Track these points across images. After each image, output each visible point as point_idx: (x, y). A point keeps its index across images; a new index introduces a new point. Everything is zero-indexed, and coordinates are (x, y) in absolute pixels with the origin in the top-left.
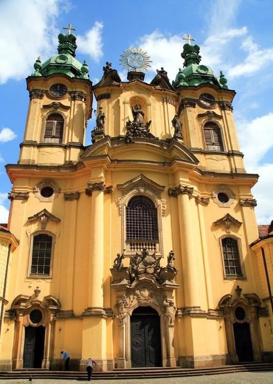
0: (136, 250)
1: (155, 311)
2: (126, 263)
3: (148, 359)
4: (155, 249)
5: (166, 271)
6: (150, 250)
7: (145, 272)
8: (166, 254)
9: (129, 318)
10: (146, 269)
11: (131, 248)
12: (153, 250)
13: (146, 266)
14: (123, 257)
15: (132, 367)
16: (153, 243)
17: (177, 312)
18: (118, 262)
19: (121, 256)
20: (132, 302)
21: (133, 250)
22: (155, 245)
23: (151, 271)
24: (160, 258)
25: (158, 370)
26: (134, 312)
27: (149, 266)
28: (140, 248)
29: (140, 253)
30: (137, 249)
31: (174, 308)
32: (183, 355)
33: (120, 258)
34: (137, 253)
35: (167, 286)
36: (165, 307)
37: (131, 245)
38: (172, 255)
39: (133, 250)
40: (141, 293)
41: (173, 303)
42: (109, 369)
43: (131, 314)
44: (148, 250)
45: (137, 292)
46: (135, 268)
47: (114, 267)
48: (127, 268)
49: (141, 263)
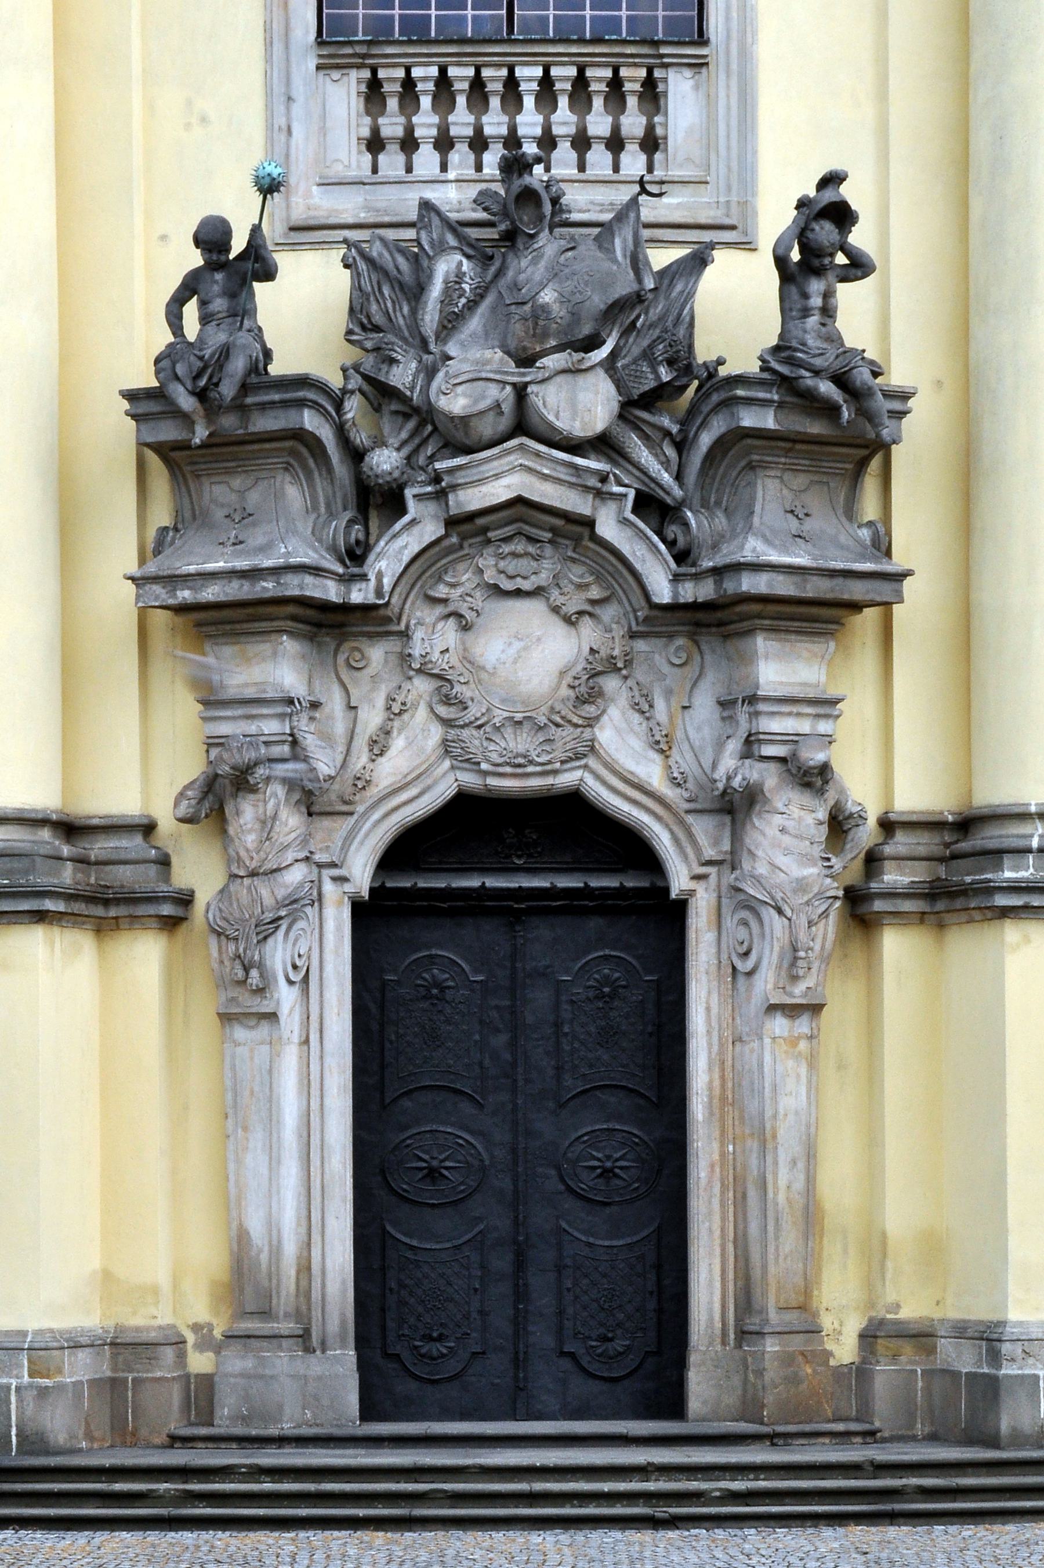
0: (426, 159)
1: (633, 850)
2: (303, 313)
3: (550, 1341)
4: (651, 143)
5: (749, 419)
6: (599, 158)
7: (523, 424)
8: (775, 218)
9: (338, 922)
10: (521, 392)
11: (375, 144)
12: (633, 162)
13: (526, 360)
14: (257, 263)
15: (368, 1412)
16: (633, 76)
17: (872, 860)
18: (205, 319)
19: (238, 244)
20: (378, 747)
21: (391, 161)
22: (652, 93)
23: (583, 401)
24: (699, 260)
25: (624, 1448)
26: (405, 851)
27: (552, 362)
28: (479, 143)
29: (455, 198)
30: (444, 143)
31: (839, 825)
32: (905, 1313)
33: (228, 268)
34: (426, 206)
35: (750, 584)
36: (735, 807)
37: (374, 93)
38: (825, 232)
39: (391, 161)
40: (467, 659)
41: (824, 770)
42: (123, 1434)
43: (361, 873)
44: (564, 154)
45: (434, 638)
46: (402, 375)
47: (165, 361)
48: (303, 381)
49: (475, 323)
